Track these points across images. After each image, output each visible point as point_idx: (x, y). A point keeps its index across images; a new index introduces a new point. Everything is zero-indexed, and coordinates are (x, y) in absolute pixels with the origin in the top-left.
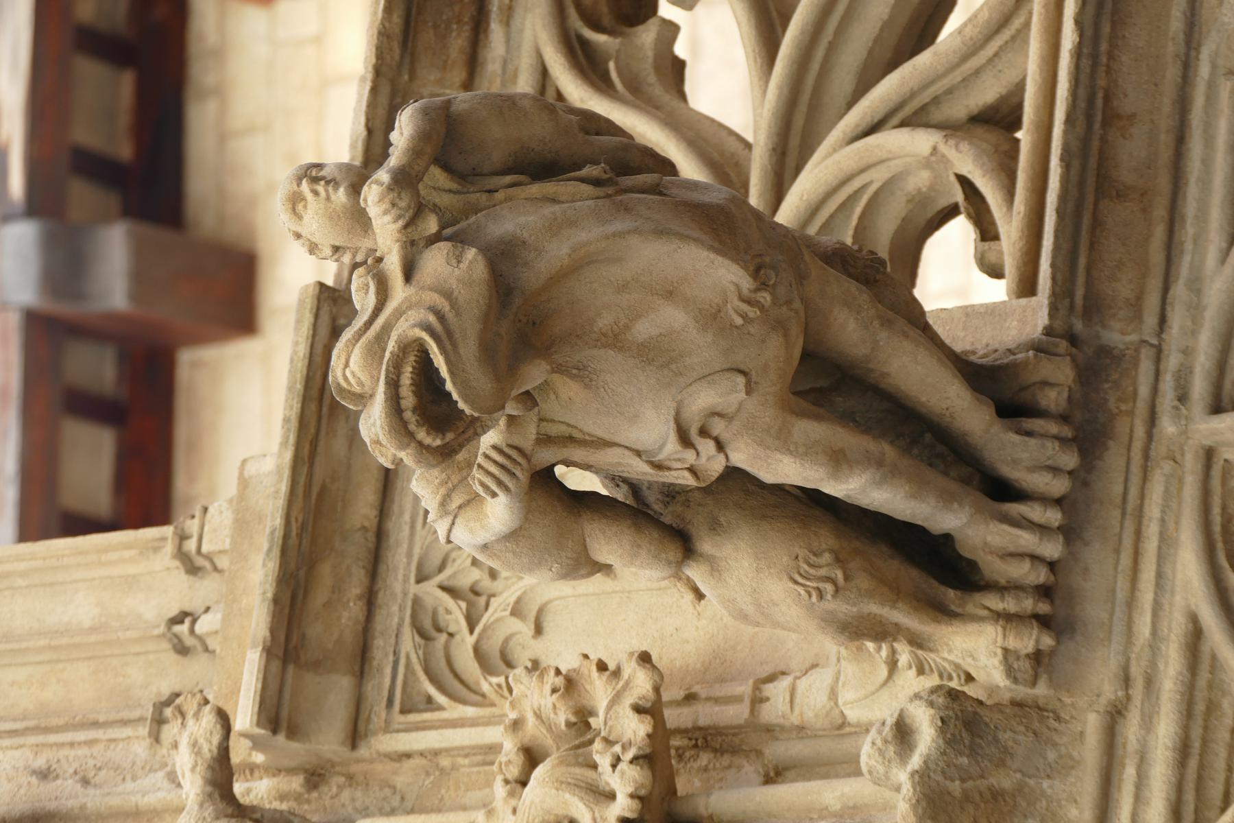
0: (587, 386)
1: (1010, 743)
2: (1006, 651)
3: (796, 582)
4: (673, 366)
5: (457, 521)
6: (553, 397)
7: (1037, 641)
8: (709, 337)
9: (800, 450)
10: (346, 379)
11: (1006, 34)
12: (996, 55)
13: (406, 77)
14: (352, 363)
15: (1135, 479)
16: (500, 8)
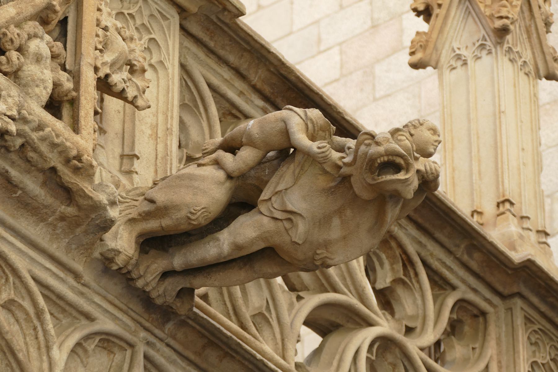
0: (324, 190)
1: (88, 236)
2: (120, 252)
3: (203, 208)
4: (318, 224)
5: (302, 121)
6: (320, 173)
7: (118, 265)
8: (321, 241)
9: (254, 241)
10: (402, 135)
11: (231, 312)
12: (225, 304)
13: (272, 69)
14: (407, 141)
15: (133, 314)
16: (267, 108)
